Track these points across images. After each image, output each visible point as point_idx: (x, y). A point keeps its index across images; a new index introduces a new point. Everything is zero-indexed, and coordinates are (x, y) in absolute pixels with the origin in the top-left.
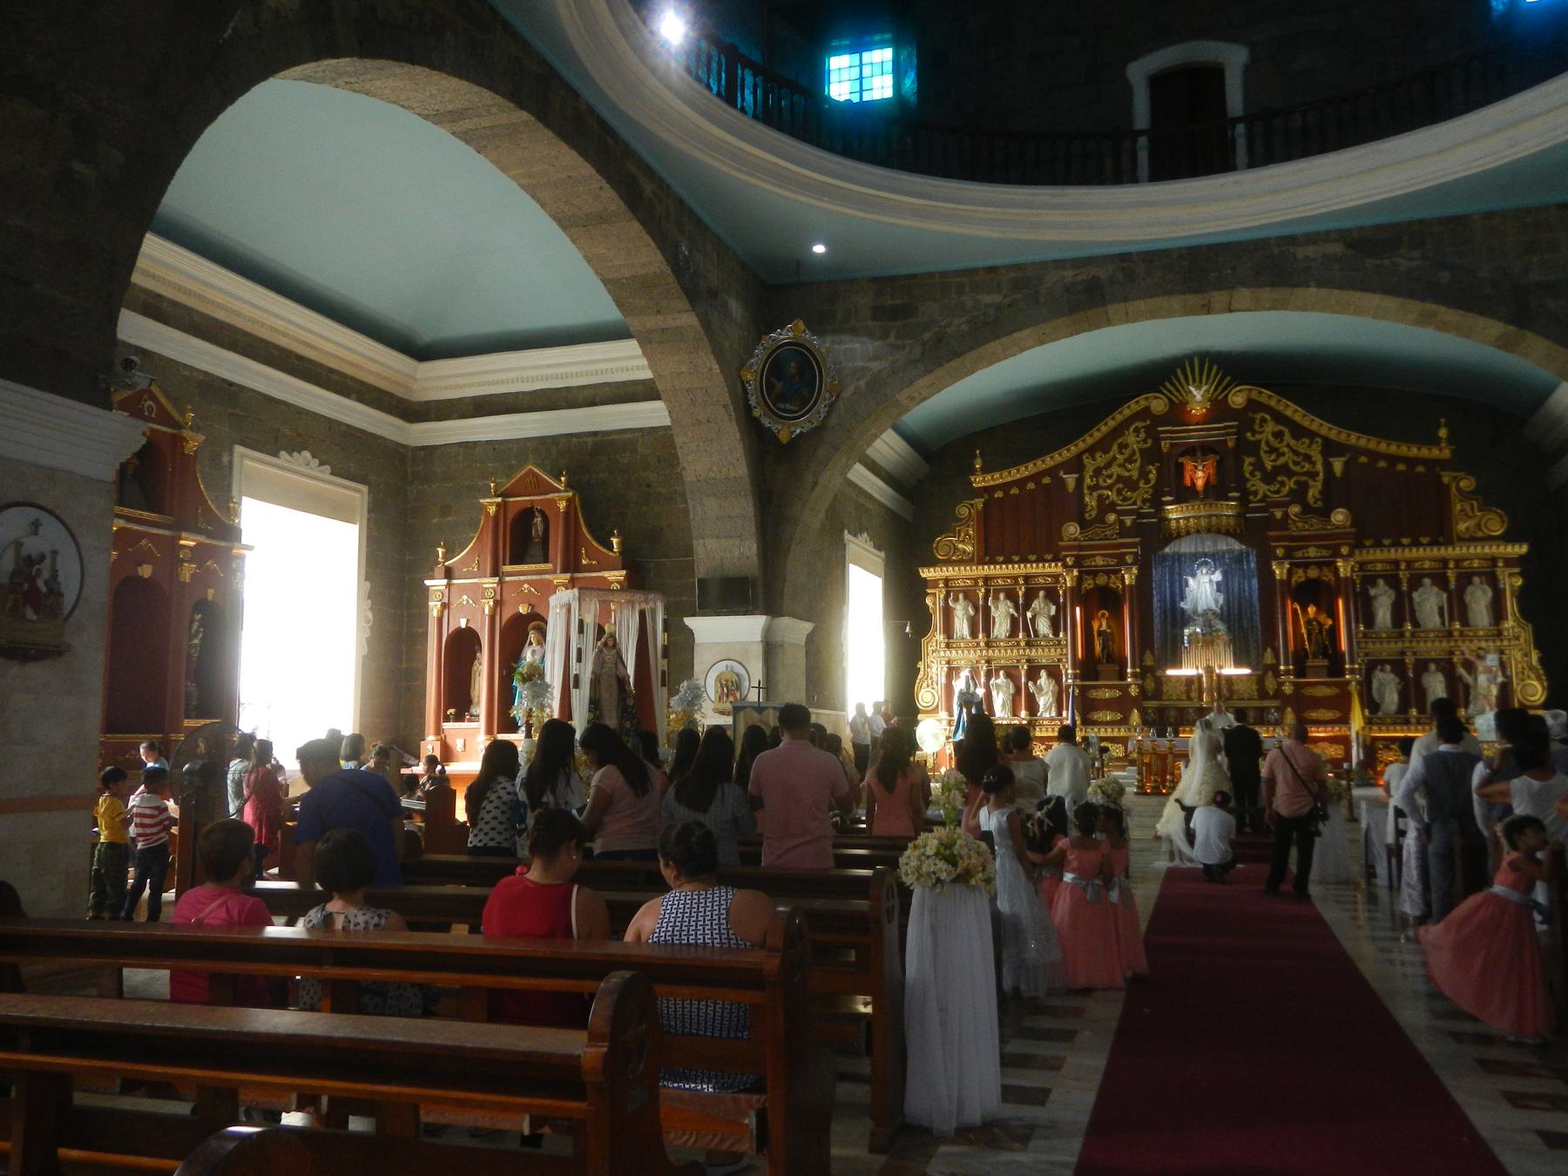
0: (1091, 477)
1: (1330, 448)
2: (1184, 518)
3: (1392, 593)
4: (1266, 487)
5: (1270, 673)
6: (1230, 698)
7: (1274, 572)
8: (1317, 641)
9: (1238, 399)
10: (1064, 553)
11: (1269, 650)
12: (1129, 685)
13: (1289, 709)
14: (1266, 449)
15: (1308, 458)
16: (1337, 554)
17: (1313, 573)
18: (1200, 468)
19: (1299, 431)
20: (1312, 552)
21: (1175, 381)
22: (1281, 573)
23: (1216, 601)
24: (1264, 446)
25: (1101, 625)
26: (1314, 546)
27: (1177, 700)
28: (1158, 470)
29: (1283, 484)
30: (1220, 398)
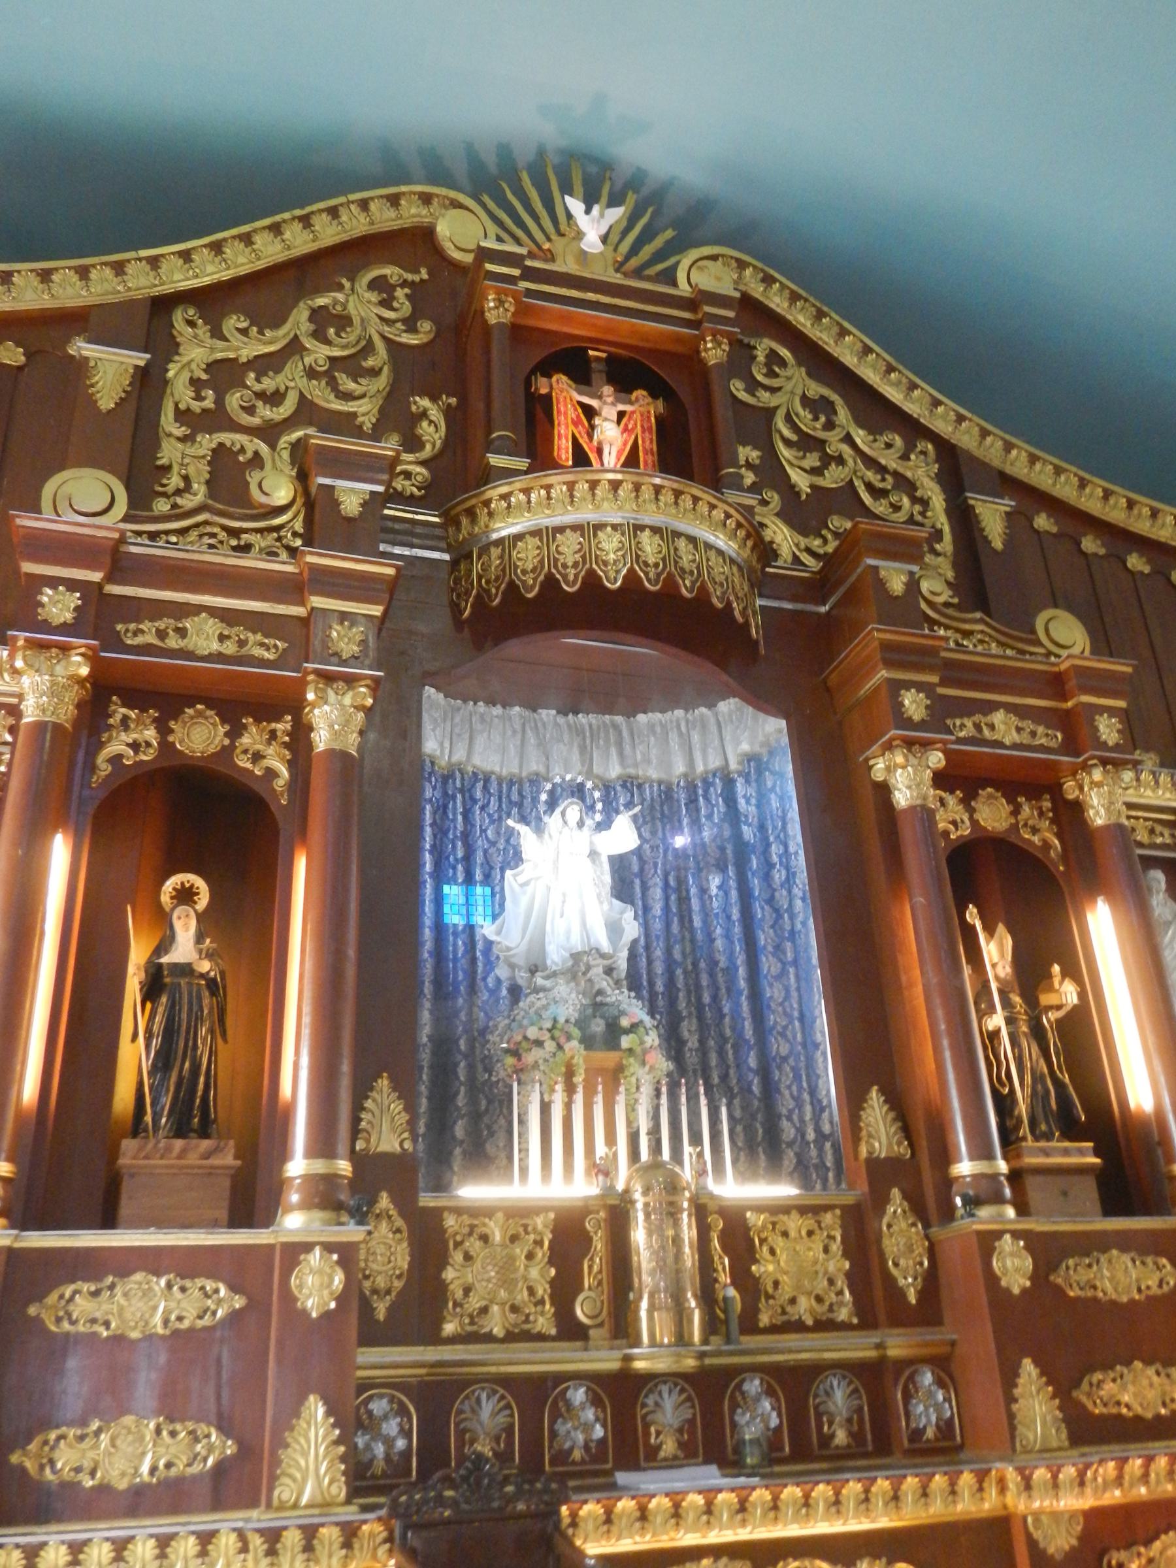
0: (195, 382)
2: (576, 528)
4: (803, 542)
5: (896, 1204)
6: (749, 1325)
7: (884, 790)
8: (1037, 1078)
10: (28, 567)
11: (875, 1097)
12: (294, 1252)
13: (1028, 1367)
14: (794, 438)
15: (907, 485)
18: (610, 412)
21: (510, 196)
23: (614, 929)
25: (165, 943)
26: (1011, 708)
27: (511, 1337)
28: (448, 412)
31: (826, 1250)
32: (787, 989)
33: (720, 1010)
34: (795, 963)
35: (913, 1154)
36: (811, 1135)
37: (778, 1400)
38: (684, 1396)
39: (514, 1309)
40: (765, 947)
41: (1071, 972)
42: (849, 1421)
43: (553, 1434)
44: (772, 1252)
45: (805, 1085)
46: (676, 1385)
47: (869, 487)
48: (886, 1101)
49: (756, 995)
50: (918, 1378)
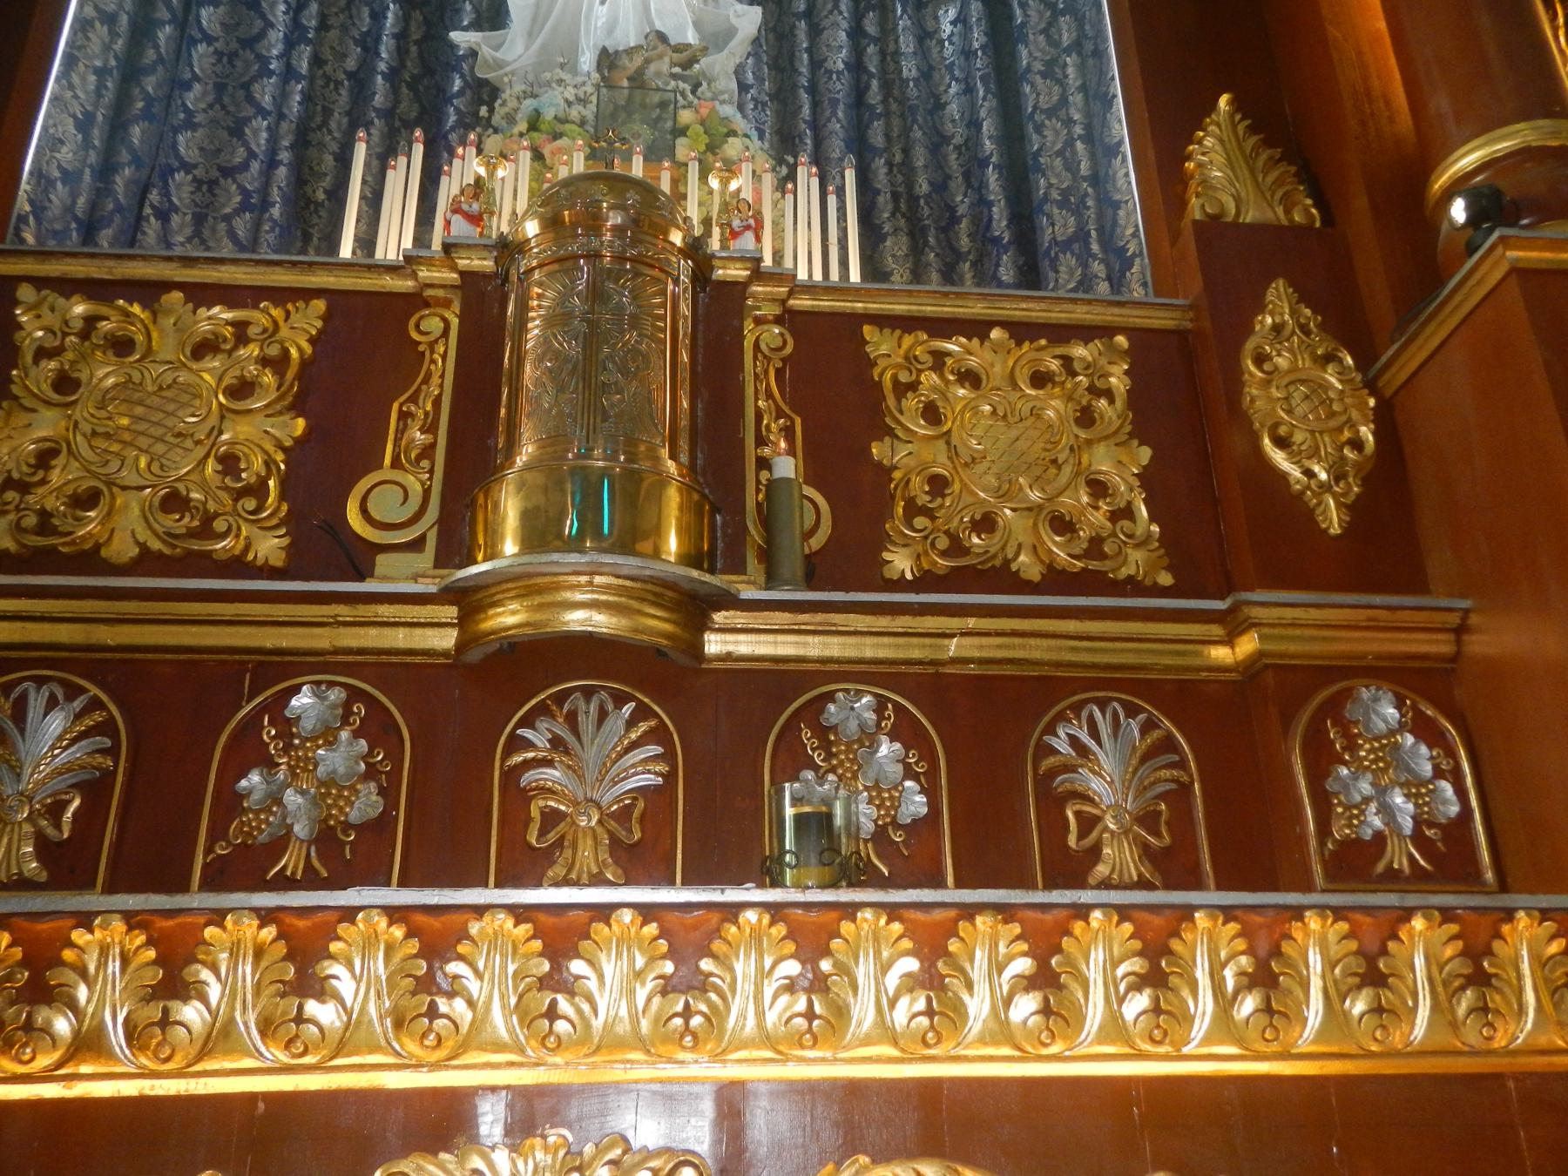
31: (1086, 418)
32: (1069, 122)
33: (952, 209)
34: (1077, 46)
35: (1327, 219)
37: (929, 755)
38: (643, 727)
39: (174, 502)
40: (1029, 69)
42: (1148, 819)
43: (231, 803)
44: (931, 414)
45: (1095, 247)
46: (620, 699)
48: (1252, 130)
49: (1019, 173)
50: (1351, 711)
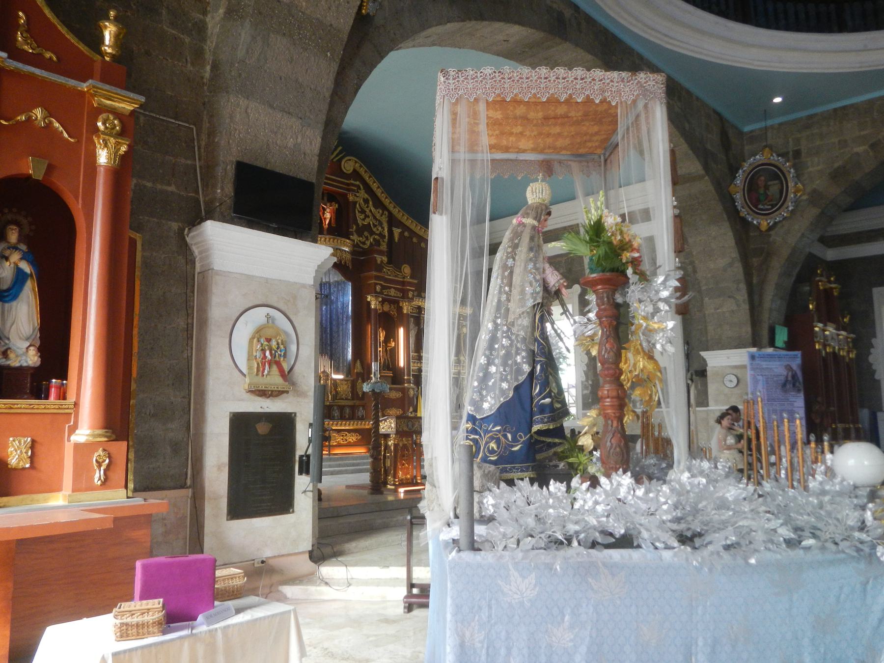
1: (393, 222)
3: (417, 327)
7: (369, 303)
9: (349, 165)
11: (358, 361)
15: (381, 224)
16: (405, 296)
17: (386, 308)
18: (328, 210)
19: (378, 204)
20: (392, 292)
22: (375, 304)
24: (358, 205)
26: (394, 288)
29: (367, 238)
30: (335, 160)
36: (341, 365)
41: (394, 341)
47: (373, 224)
